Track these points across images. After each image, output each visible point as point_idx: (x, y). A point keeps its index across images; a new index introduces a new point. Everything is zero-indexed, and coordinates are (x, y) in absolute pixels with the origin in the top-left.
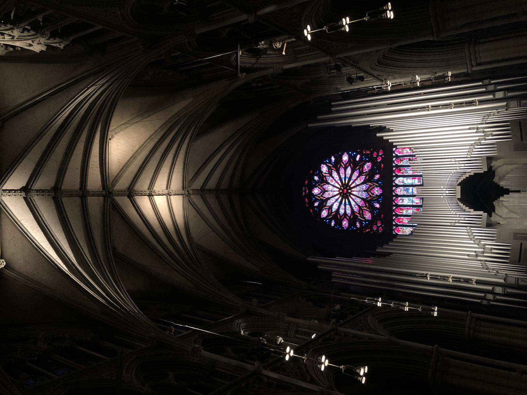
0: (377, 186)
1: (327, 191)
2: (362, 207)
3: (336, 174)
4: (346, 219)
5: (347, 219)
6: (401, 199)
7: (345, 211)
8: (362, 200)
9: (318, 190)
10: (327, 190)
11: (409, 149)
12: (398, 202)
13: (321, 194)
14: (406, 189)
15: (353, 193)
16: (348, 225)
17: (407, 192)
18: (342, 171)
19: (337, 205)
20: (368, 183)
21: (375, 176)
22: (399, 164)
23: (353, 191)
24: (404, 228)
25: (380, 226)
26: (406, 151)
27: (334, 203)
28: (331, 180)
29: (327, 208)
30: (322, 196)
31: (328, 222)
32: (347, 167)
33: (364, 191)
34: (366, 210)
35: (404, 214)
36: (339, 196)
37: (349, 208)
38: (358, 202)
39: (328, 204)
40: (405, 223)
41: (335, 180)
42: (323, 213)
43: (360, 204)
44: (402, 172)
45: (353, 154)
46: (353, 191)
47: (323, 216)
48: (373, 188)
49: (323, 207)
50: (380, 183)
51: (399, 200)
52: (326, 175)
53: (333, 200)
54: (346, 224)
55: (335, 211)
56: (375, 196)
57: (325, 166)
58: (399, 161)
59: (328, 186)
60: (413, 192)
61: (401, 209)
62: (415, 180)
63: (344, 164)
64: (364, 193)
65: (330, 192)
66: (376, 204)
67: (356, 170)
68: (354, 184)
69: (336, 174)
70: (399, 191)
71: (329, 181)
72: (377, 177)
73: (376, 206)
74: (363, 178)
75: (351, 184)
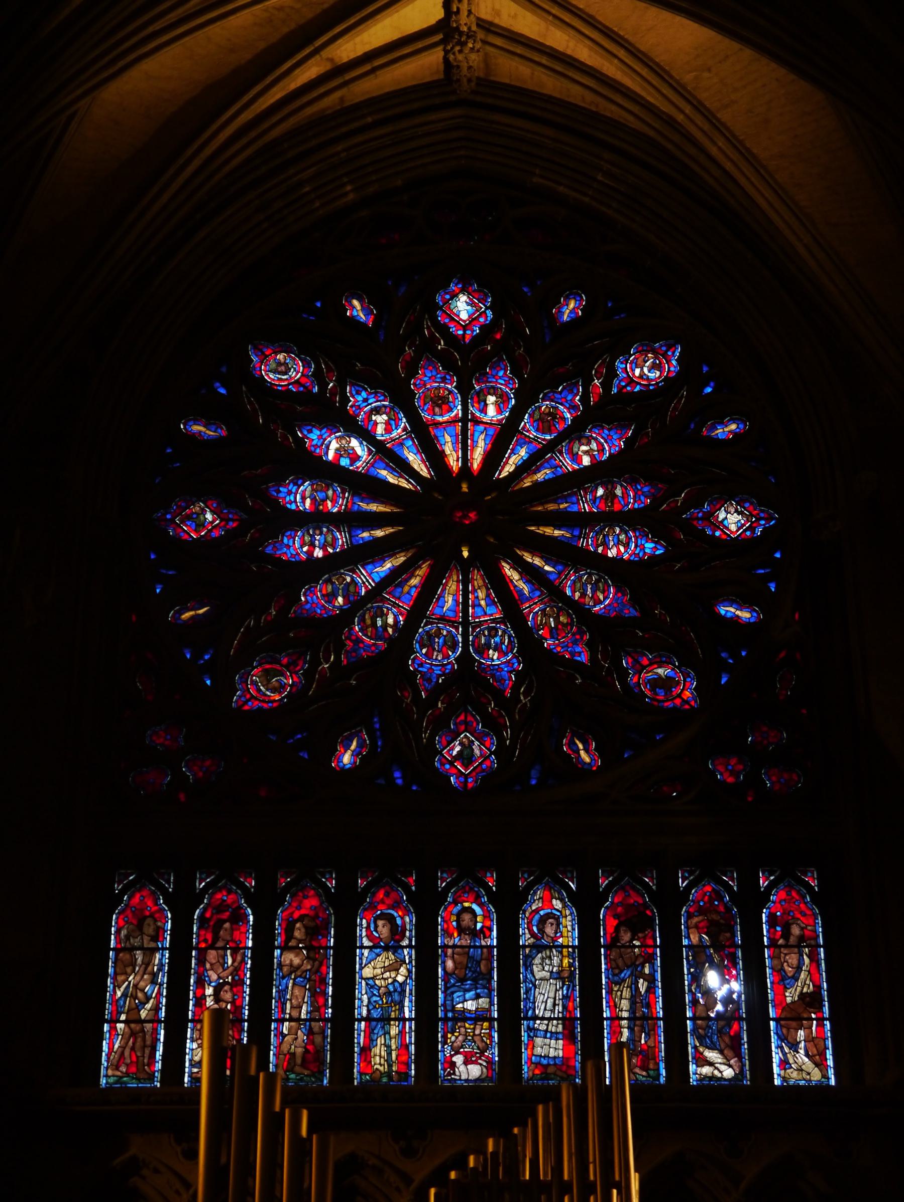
1: (465, 390)
2: (339, 647)
3: (601, 450)
6: (397, 933)
9: (473, 320)
11: (809, 988)
12: (373, 907)
14: (483, 967)
16: (184, 536)
17: (462, 980)
19: (355, 458)
20: (526, 694)
22: (689, 916)
24: (161, 958)
26: (799, 969)
27: (367, 436)
28: (554, 415)
29: (323, 386)
32: (657, 536)
33: (466, 658)
34: (309, 675)
35: (277, 952)
37: (323, 547)
39: (360, 398)
40: (201, 961)
41: (551, 446)
44: (626, 937)
45: (767, 579)
48: (493, 725)
51: (391, 919)
53: (388, 430)
54: (201, 525)
57: (673, 366)
58: (715, 917)
60: (455, 1020)
61: (316, 931)
62: (555, 1036)
65: (458, 410)
66: (361, 745)
68: (525, 589)
69: (601, 450)
70: (467, 917)
73: (347, 748)
74: (573, 654)
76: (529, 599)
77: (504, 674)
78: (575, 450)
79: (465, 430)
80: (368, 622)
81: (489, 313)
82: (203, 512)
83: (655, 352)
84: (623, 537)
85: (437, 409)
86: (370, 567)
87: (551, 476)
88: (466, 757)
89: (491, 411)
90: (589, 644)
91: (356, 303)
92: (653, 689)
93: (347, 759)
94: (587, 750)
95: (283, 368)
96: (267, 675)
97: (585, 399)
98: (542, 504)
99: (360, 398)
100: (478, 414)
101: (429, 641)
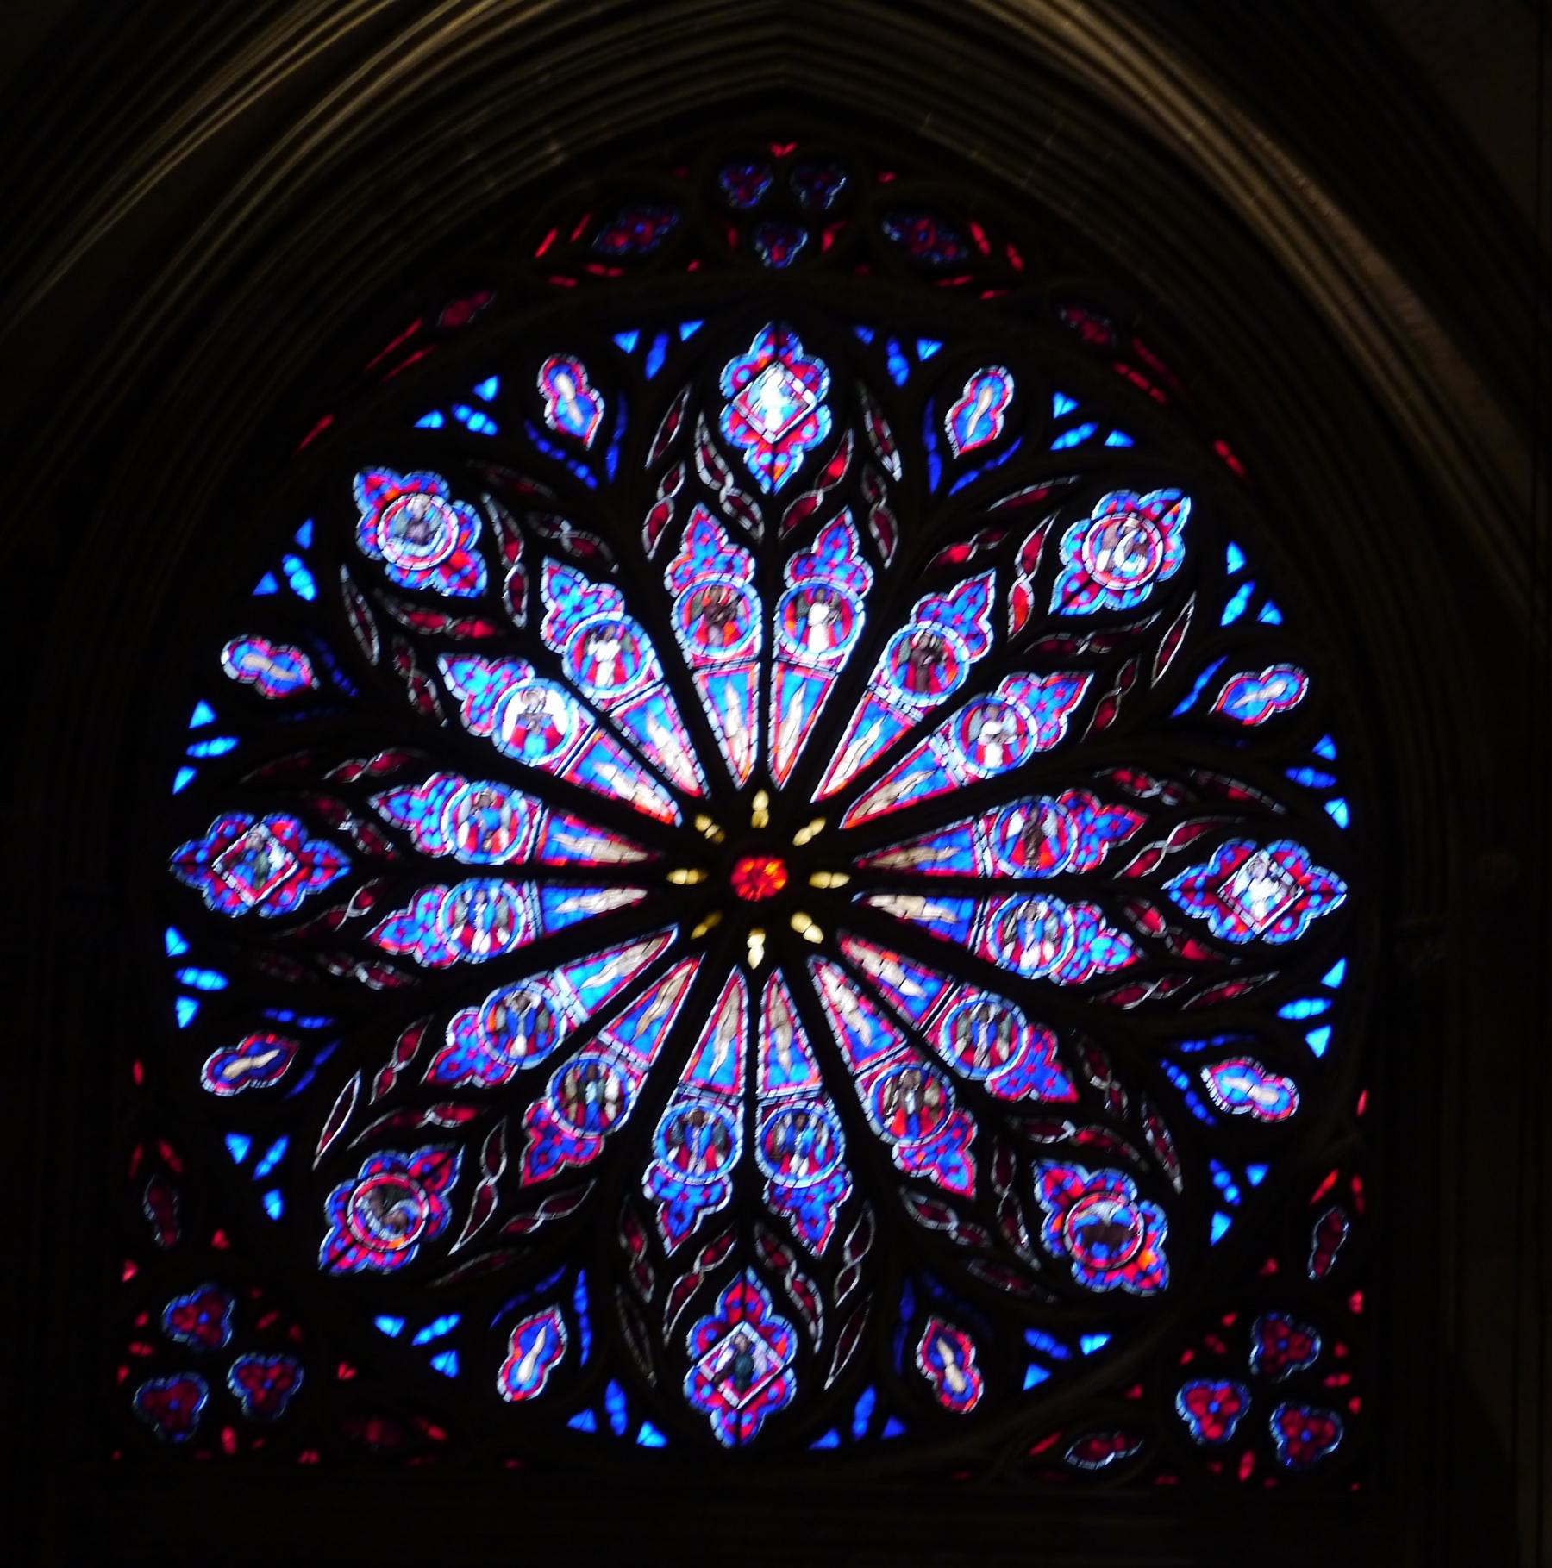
0: (808, 1365)
1: (768, 585)
2: (517, 1140)
3: (1022, 731)
4: (321, 881)
5: (339, 893)
7: (448, 872)
8: (613, 1141)
9: (792, 433)
10: (792, 585)
13: (728, 488)
15: (728, 1018)
18: (1062, 836)
19: (554, 739)
20: (856, 1248)
21: (957, 1349)
23: (755, 1011)
25: (223, 1402)
28: (938, 654)
29: (496, 573)
30: (696, 492)
31: (283, 579)
33: (746, 1175)
34: (460, 1198)
36: (687, 773)
37: (492, 931)
38: (581, 1084)
39: (567, 604)
41: (932, 720)
42: (417, 503)
43: (549, 1103)
46: (755, 1011)
47: (383, 504)
49: (512, 502)
50: (864, 1406)
52: (1024, 581)
53: (620, 678)
55: (451, 704)
56: (668, 1329)
59: (844, 611)
63: (1173, 865)
64: (712, 1167)
65: (755, 637)
66: (553, 1345)
67: (1067, 1061)
69: (1022, 731)
71: (920, 629)
72: (940, 1369)
73: (526, 1349)
74: (946, 1170)
75: (856, 976)
76: (872, 1052)
77: (817, 1207)
78: (973, 733)
79: (765, 681)
80: (571, 1091)
81: (824, 415)
82: (265, 846)
83: (1142, 514)
84: (1051, 925)
85: (714, 633)
86: (576, 974)
87: (925, 790)
88: (740, 1374)
89: (819, 636)
90: (980, 1150)
91: (563, 383)
92: (1087, 1245)
93: (525, 1371)
94: (961, 1365)
95: (418, 531)
96: (385, 1195)
97: (998, 619)
98: (906, 848)
99: (567, 604)
100: (791, 647)
101: (680, 1137)
